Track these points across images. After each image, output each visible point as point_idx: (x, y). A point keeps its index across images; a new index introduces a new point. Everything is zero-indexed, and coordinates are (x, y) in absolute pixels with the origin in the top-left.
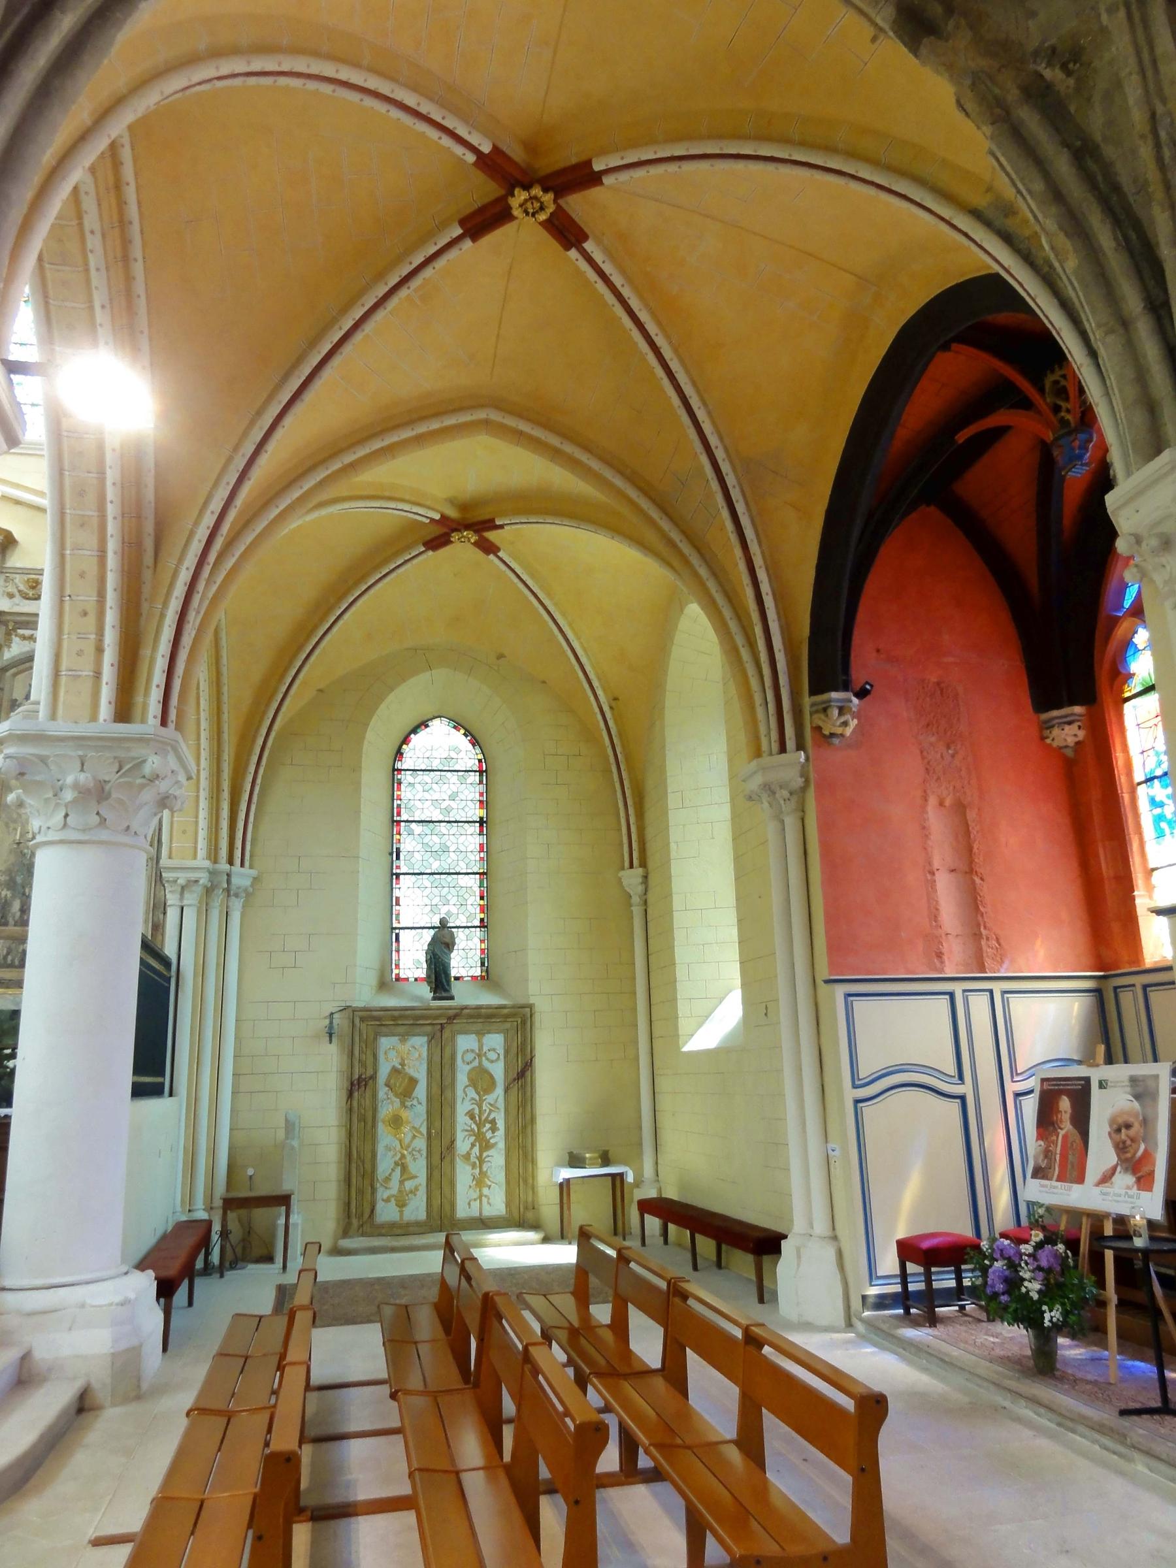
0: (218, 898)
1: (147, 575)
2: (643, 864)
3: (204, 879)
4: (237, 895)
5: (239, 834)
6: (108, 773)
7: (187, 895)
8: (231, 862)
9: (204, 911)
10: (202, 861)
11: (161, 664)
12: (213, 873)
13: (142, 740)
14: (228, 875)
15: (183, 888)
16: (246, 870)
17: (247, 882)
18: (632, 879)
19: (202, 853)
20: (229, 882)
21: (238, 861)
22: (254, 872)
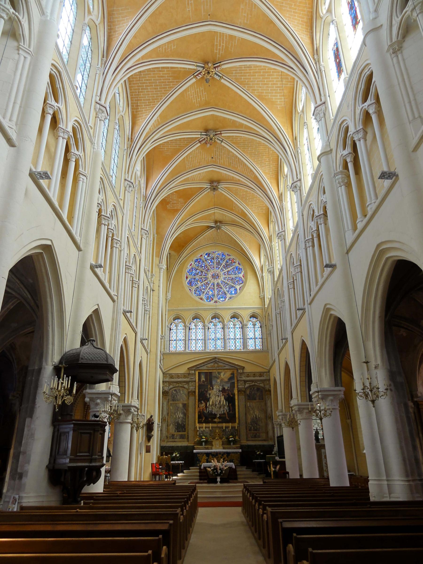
2: (351, 419)
18: (349, 421)
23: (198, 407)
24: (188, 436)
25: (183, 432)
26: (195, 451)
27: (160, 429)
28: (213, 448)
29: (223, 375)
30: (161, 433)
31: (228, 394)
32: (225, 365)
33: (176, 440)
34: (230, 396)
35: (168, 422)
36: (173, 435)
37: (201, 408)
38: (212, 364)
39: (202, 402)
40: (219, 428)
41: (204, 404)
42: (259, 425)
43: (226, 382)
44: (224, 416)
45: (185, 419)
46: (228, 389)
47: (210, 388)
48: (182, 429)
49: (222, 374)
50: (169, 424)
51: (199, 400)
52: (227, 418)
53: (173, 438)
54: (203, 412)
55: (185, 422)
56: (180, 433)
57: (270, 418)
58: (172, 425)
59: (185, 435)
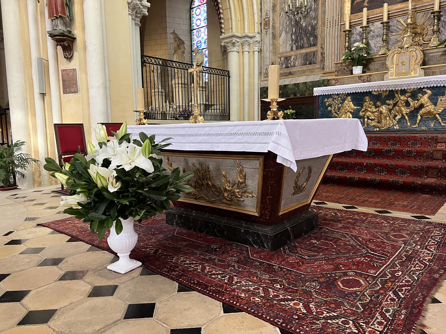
24: (322, 54)
25: (310, 46)
26: (317, 91)
27: (256, 49)
28: (389, 76)
30: (261, 59)
33: (293, 70)
35: (274, 27)
36: (287, 59)
45: (316, 10)
48: (308, 40)
50: (278, 32)
53: (287, 67)
55: (316, 18)
56: (304, 51)
58: (283, 34)
59: (314, 53)
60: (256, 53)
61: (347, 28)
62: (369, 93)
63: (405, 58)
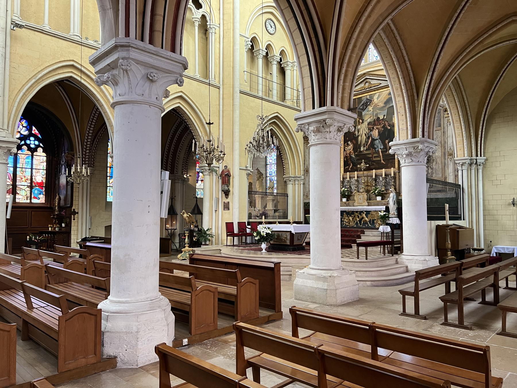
0: (474, 167)
1: (416, 101)
3: (468, 161)
4: (480, 165)
5: (479, 147)
6: (412, 150)
7: (463, 167)
8: (477, 156)
9: (469, 170)
10: (466, 157)
11: (421, 122)
12: (471, 160)
13: (418, 142)
14: (476, 160)
15: (462, 165)
16: (482, 157)
17: (483, 161)
19: (466, 155)
20: (476, 162)
21: (479, 155)
22: (485, 158)
23: (344, 150)
28: (356, 204)
29: (378, 98)
31: (384, 127)
32: (381, 82)
34: (387, 128)
37: (348, 152)
38: (362, 85)
39: (349, 142)
40: (368, 176)
41: (351, 146)
42: (432, 169)
43: (382, 109)
44: (379, 159)
46: (383, 119)
47: (359, 121)
49: (375, 97)
51: (346, 141)
52: (382, 161)
54: (351, 157)
57: (451, 155)
60: (302, 185)
61: (342, 180)
62: (345, 211)
63: (361, 196)
